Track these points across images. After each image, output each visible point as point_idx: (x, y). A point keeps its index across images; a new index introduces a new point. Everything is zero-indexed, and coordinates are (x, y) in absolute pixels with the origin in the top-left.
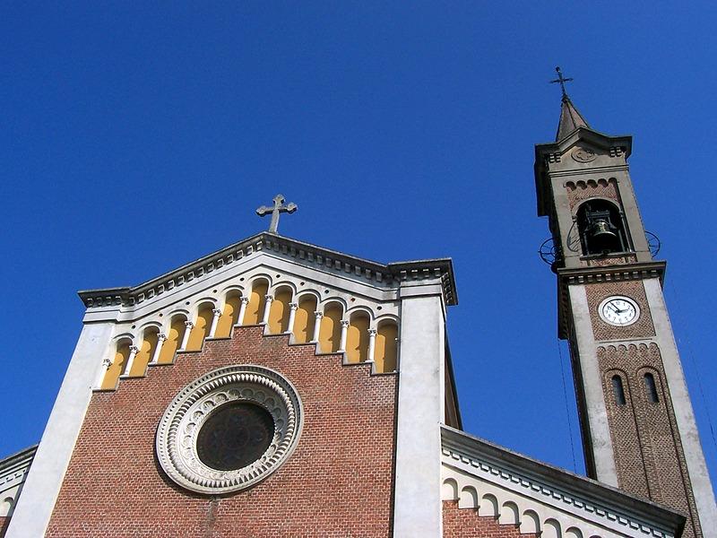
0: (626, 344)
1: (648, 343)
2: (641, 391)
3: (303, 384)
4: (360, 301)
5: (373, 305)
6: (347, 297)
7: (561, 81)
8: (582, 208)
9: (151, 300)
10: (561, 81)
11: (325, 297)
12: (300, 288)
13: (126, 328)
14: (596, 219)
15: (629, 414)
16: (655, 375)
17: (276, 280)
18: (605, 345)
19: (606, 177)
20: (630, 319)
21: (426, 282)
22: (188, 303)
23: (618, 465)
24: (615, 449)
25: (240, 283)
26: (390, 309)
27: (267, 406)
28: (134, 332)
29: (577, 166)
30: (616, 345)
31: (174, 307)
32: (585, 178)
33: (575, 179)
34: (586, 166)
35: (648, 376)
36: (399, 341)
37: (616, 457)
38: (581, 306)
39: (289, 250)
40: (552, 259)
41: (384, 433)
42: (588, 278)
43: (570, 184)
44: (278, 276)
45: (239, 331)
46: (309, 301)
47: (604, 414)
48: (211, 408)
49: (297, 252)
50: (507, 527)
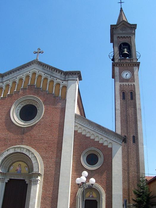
0: (127, 84)
1: (132, 84)
2: (128, 97)
4: (58, 80)
5: (61, 81)
7: (121, 3)
8: (121, 45)
9: (7, 77)
10: (121, 3)
12: (44, 76)
14: (124, 48)
16: (133, 92)
18: (122, 84)
19: (128, 36)
20: (129, 77)
21: (74, 76)
22: (16, 78)
24: (121, 111)
25: (29, 73)
28: (3, 85)
29: (121, 32)
30: (125, 84)
32: (123, 36)
33: (120, 36)
34: (124, 32)
36: (67, 91)
37: (121, 113)
38: (117, 73)
39: (41, 65)
40: (112, 58)
43: (118, 37)
44: (39, 72)
45: (29, 86)
46: (46, 79)
47: (119, 102)
48: (22, 106)
49: (43, 66)
50: (87, 137)
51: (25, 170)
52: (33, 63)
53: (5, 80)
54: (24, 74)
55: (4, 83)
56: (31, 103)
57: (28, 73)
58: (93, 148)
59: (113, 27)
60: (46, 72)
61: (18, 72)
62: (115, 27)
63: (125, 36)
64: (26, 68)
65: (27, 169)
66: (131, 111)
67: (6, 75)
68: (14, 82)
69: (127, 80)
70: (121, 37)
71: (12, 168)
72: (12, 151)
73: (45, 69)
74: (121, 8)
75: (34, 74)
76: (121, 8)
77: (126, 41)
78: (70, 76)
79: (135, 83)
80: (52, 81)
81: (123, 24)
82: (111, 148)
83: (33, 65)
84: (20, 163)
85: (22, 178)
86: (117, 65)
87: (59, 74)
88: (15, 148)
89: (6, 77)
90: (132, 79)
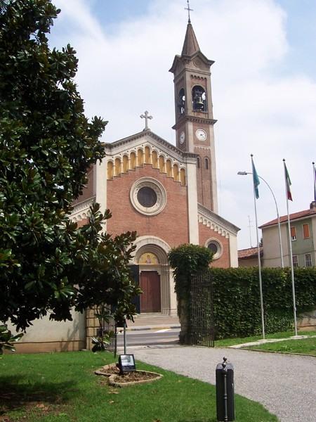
2: (204, 165)
3: (165, 186)
4: (176, 161)
6: (173, 159)
7: (189, 9)
11: (167, 157)
13: (110, 158)
19: (204, 76)
26: (183, 166)
27: (155, 190)
29: (194, 68)
32: (197, 75)
33: (194, 74)
35: (206, 160)
41: (185, 203)
42: (195, 120)
43: (192, 76)
46: (162, 157)
51: (154, 262)
53: (113, 153)
55: (114, 156)
57: (141, 146)
58: (214, 239)
60: (162, 149)
61: (129, 143)
65: (156, 260)
66: (206, 183)
67: (115, 146)
68: (125, 156)
69: (202, 143)
70: (195, 76)
71: (140, 259)
72: (145, 243)
74: (189, 22)
75: (147, 148)
76: (189, 22)
77: (201, 83)
80: (168, 161)
81: (198, 56)
82: (229, 239)
83: (145, 137)
84: (148, 254)
85: (154, 270)
89: (115, 151)
90: (208, 142)
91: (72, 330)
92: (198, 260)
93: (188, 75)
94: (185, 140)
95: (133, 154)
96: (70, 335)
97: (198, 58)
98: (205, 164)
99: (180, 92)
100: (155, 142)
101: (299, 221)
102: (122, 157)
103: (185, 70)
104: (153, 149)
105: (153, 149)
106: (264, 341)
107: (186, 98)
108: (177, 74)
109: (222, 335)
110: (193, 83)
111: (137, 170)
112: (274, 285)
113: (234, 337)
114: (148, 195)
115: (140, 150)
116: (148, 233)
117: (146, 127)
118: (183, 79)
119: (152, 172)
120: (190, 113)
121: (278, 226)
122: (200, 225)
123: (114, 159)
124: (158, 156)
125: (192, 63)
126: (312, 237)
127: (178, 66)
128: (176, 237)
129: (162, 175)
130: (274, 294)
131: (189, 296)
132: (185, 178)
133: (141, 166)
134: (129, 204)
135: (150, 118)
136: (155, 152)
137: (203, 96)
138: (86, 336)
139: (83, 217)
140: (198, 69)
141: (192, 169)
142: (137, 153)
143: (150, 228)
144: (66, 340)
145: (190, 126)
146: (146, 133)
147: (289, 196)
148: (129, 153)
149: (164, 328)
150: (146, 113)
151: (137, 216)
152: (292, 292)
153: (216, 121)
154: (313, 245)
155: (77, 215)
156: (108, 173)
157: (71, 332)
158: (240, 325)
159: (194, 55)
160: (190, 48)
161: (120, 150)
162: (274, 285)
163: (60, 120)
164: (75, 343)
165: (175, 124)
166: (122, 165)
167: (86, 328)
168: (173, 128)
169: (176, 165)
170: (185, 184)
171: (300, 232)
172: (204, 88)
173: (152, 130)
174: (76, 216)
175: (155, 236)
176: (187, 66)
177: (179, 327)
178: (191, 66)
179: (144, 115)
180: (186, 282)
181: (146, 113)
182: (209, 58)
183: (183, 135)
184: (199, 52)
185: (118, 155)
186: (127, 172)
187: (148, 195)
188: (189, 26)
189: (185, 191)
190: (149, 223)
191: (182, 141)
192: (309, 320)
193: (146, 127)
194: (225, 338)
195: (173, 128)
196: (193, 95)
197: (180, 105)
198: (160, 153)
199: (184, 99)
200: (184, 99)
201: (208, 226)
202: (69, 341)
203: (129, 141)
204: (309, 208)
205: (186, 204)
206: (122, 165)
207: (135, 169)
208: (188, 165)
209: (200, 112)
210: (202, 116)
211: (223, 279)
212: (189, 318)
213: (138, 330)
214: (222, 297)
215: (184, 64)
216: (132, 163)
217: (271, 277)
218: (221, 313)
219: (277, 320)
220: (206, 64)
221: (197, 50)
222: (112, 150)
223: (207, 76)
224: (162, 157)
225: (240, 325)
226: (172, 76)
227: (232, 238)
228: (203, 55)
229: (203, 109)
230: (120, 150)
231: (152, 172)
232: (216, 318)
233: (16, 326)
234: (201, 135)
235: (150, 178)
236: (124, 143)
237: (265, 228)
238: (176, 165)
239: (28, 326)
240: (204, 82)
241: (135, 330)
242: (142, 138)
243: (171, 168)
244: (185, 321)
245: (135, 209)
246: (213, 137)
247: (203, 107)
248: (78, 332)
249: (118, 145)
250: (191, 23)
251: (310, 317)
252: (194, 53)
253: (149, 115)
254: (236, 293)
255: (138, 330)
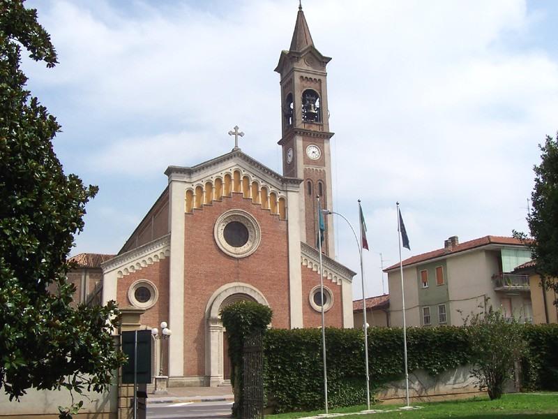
0: (315, 169)
1: (322, 170)
2: (316, 191)
4: (273, 189)
5: (278, 191)
6: (269, 186)
11: (262, 184)
13: (189, 186)
15: (311, 200)
16: (323, 185)
17: (244, 173)
19: (317, 77)
23: (306, 220)
26: (282, 194)
29: (305, 67)
31: (207, 179)
32: (309, 76)
33: (305, 75)
37: (306, 216)
42: (306, 134)
43: (302, 77)
46: (255, 183)
52: (235, 156)
54: (223, 172)
55: (195, 184)
56: (239, 221)
57: (228, 170)
59: (297, 56)
61: (213, 167)
62: (297, 56)
63: (313, 77)
64: (225, 163)
67: (196, 171)
69: (314, 162)
70: (306, 77)
73: (253, 167)
74: (300, 8)
75: (237, 172)
76: (300, 8)
77: (313, 87)
78: (290, 185)
79: (325, 169)
80: (264, 189)
81: (310, 52)
82: (341, 286)
83: (234, 158)
86: (300, 133)
87: (274, 180)
88: (236, 287)
89: (195, 177)
90: (322, 161)
91: (101, 401)
92: (252, 320)
93: (297, 76)
94: (293, 158)
95: (219, 180)
96: (99, 407)
97: (309, 54)
98: (317, 189)
99: (288, 98)
100: (246, 165)
101: (428, 264)
102: (204, 184)
103: (293, 70)
104: (243, 173)
105: (243, 173)
106: (369, 411)
107: (294, 106)
108: (284, 75)
109: (282, 408)
110: (304, 87)
111: (224, 201)
112: (350, 349)
113: (298, 411)
114: (237, 232)
115: (228, 176)
116: (237, 279)
117: (236, 146)
118: (291, 82)
119: (242, 202)
120: (300, 123)
121: (400, 270)
122: (304, 269)
123: (194, 188)
124: (251, 183)
125: (302, 61)
126: (447, 284)
127: (286, 64)
128: (273, 285)
129: (255, 207)
130: (349, 360)
131: (241, 362)
132: (284, 209)
133: (228, 197)
134: (213, 242)
135: (241, 135)
136: (246, 178)
137: (317, 104)
138: (118, 407)
139: (155, 260)
140: (310, 68)
141: (296, 200)
142: (223, 180)
143: (238, 274)
144: (95, 412)
145: (299, 142)
146: (236, 154)
147: (365, 245)
148: (214, 180)
149: (183, 401)
150: (236, 128)
151: (223, 259)
152: (404, 351)
153: (333, 134)
154: (448, 293)
155: (123, 268)
156: (187, 205)
157: (99, 404)
158: (307, 396)
159: (304, 51)
160: (301, 42)
161: (201, 176)
162: (350, 349)
163: (24, 199)
164: (105, 415)
165: (281, 138)
166: (195, 198)
167: (118, 398)
168: (279, 143)
169: (273, 194)
170: (284, 217)
171: (432, 278)
172: (318, 92)
173: (244, 150)
174: (146, 259)
175: (246, 282)
176: (296, 66)
177: (231, 399)
178: (302, 66)
179: (234, 131)
180: (237, 345)
181: (236, 128)
182: (324, 54)
183: (291, 153)
184: (312, 47)
185: (200, 182)
186: (210, 204)
187: (237, 232)
188: (301, 14)
189: (285, 226)
190: (238, 267)
191: (290, 160)
192: (396, 391)
193: (236, 146)
194: (286, 411)
195: (279, 143)
196: (304, 101)
197: (287, 114)
198: (253, 179)
199: (292, 107)
200: (292, 107)
201: (314, 269)
202: (97, 413)
203: (214, 164)
204: (444, 247)
205: (286, 244)
206: (205, 194)
207: (220, 199)
208: (289, 193)
209: (312, 123)
210: (314, 128)
211: (284, 342)
212: (241, 386)
213: (209, 401)
214: (283, 363)
215: (292, 62)
216: (218, 192)
217: (346, 339)
218: (281, 382)
219: (353, 391)
220: (320, 62)
221: (309, 45)
222: (192, 176)
223: (321, 78)
224: (255, 183)
225: (307, 396)
226: (278, 76)
227: (345, 286)
228: (316, 50)
229: (317, 121)
230: (201, 176)
231: (242, 202)
232: (273, 388)
233: (9, 395)
234: (313, 152)
235: (238, 210)
236: (207, 167)
237: (392, 272)
238: (273, 194)
239: (22, 395)
240: (317, 84)
241: (206, 401)
242: (231, 160)
243: (267, 198)
244: (238, 390)
245: (221, 250)
246: (330, 155)
247: (316, 117)
248: (109, 402)
249: (200, 170)
250: (303, 10)
251: (399, 387)
252: (306, 47)
253: (239, 131)
254: (301, 359)
255: (209, 401)
